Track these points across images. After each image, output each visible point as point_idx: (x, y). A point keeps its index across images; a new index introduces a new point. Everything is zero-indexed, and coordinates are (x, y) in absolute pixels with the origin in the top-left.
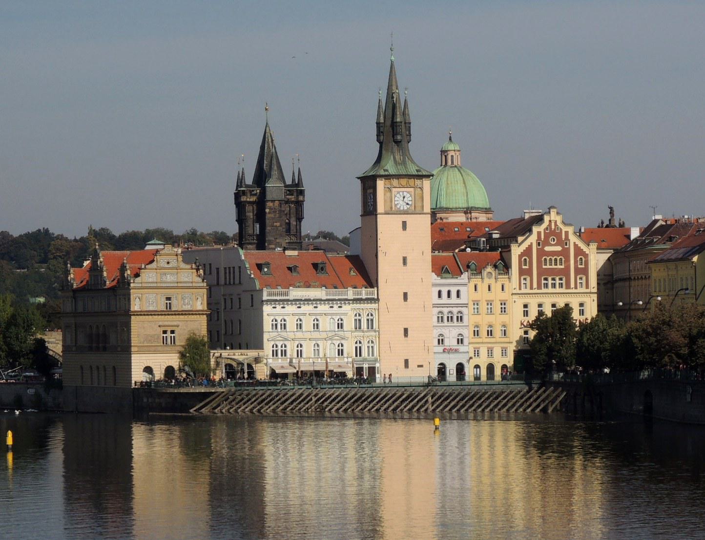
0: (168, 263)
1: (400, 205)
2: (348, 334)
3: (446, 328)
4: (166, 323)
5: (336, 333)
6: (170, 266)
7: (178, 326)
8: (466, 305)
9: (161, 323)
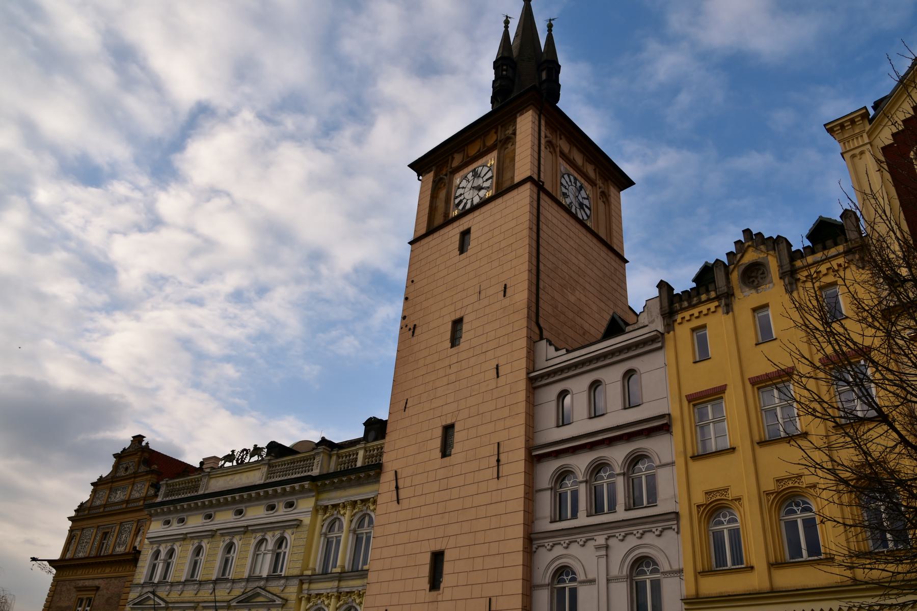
0: (126, 469)
1: (465, 201)
2: (292, 591)
3: (581, 538)
4: (87, 583)
5: (262, 583)
6: (129, 472)
7: (97, 588)
8: (661, 426)
9: (81, 583)
